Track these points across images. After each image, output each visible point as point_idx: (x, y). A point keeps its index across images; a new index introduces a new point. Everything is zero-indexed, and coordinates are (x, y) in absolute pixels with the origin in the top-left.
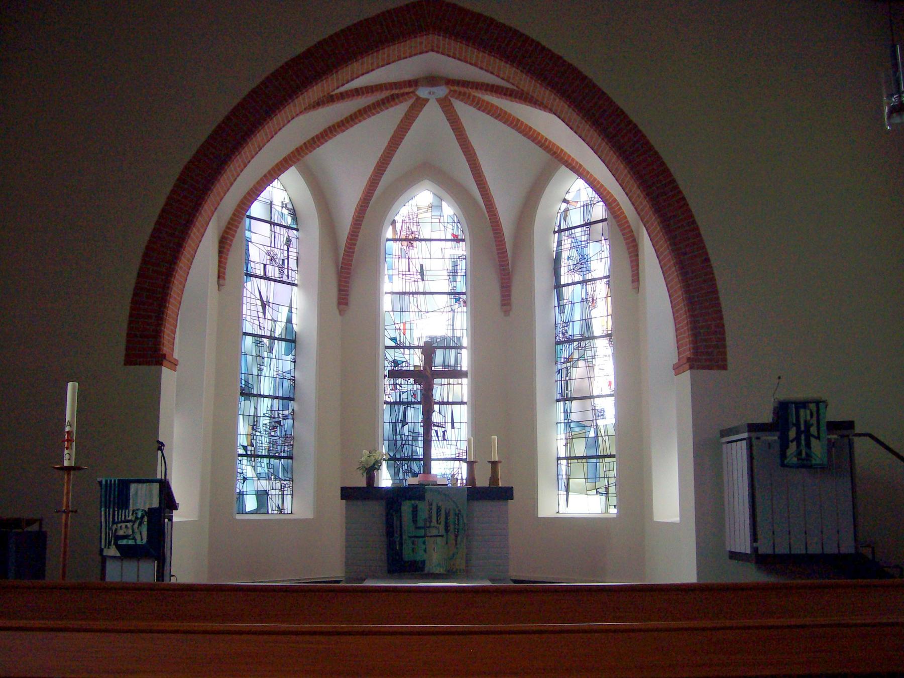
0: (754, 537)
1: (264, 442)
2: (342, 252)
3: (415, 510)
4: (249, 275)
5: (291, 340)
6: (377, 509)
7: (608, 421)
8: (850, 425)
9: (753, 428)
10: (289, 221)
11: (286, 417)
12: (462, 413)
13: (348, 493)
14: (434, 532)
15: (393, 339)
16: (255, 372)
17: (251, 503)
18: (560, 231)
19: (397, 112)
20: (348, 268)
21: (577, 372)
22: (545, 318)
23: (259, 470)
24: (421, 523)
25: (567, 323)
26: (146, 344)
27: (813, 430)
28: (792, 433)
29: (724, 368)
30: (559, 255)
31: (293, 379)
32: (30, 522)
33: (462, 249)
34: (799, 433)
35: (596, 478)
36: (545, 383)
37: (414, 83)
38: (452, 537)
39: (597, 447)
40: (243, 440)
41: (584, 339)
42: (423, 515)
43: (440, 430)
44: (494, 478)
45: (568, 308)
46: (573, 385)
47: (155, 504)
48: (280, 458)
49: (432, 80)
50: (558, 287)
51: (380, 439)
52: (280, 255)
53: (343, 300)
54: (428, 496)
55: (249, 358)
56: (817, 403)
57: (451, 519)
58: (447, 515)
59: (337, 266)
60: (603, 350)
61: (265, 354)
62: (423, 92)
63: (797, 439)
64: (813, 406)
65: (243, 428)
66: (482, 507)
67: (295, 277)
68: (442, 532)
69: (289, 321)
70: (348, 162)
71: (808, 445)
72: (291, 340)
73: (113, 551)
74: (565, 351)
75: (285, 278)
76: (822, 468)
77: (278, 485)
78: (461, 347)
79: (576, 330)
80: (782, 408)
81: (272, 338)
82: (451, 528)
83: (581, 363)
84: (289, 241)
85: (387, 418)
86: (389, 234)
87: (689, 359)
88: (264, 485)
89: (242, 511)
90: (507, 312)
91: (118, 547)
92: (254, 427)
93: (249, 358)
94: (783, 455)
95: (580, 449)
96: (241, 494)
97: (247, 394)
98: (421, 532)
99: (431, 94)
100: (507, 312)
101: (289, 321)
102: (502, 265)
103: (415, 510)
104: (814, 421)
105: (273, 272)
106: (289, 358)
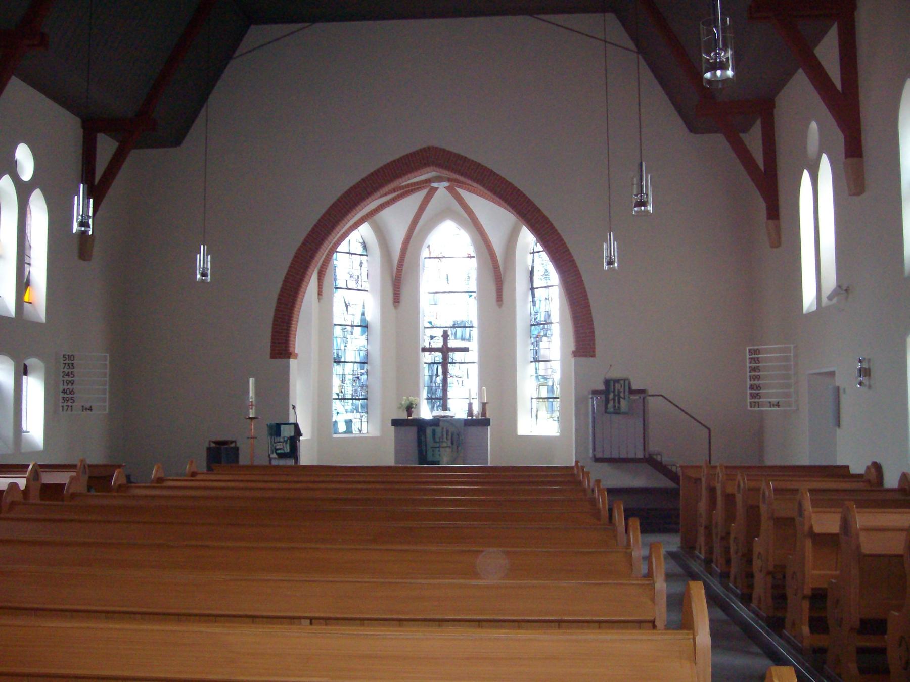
0: (594, 450)
1: (349, 391)
2: (395, 270)
3: (434, 432)
4: (336, 288)
5: (365, 326)
6: (412, 432)
7: (557, 377)
8: (642, 391)
9: (595, 392)
10: (360, 250)
11: (362, 374)
12: (474, 370)
13: (396, 423)
14: (445, 444)
15: (430, 323)
16: (343, 348)
17: (342, 427)
18: (534, 253)
19: (422, 194)
20: (399, 281)
21: (544, 344)
22: (523, 310)
23: (347, 407)
24: (437, 440)
25: (537, 313)
26: (281, 346)
27: (622, 395)
28: (611, 396)
29: (594, 356)
30: (533, 268)
31: (367, 351)
32: (232, 442)
33: (474, 263)
34: (615, 395)
35: (552, 411)
36: (523, 350)
37: (428, 181)
38: (455, 446)
39: (553, 392)
40: (335, 389)
41: (547, 324)
42: (438, 435)
43: (460, 380)
44: (484, 413)
45: (537, 303)
46: (542, 352)
47: (292, 434)
48: (359, 399)
49: (439, 179)
50: (532, 289)
51: (421, 385)
52: (356, 273)
53: (397, 300)
54: (441, 424)
55: (339, 340)
56: (625, 380)
57: (455, 437)
58: (452, 435)
59: (392, 277)
60: (555, 329)
61: (349, 336)
62: (434, 185)
63: (614, 399)
64: (622, 382)
65: (336, 382)
66: (473, 430)
67: (366, 286)
68: (449, 443)
69: (363, 314)
70: (397, 217)
71: (619, 402)
72: (365, 326)
73: (274, 455)
74: (536, 331)
75: (359, 288)
76: (625, 413)
77: (358, 415)
78: (472, 327)
79: (542, 318)
80: (607, 382)
81: (352, 326)
82: (455, 443)
83: (544, 339)
84: (361, 264)
85: (426, 372)
86: (425, 253)
87: (573, 352)
88: (350, 416)
89: (336, 432)
90: (500, 306)
91: (278, 454)
92: (343, 381)
93: (339, 340)
94: (606, 408)
95: (544, 394)
96: (336, 422)
97: (338, 362)
98: (437, 445)
99: (442, 187)
100: (500, 306)
101: (363, 314)
102: (497, 276)
103: (434, 432)
104: (622, 390)
105: (352, 285)
106: (365, 337)
